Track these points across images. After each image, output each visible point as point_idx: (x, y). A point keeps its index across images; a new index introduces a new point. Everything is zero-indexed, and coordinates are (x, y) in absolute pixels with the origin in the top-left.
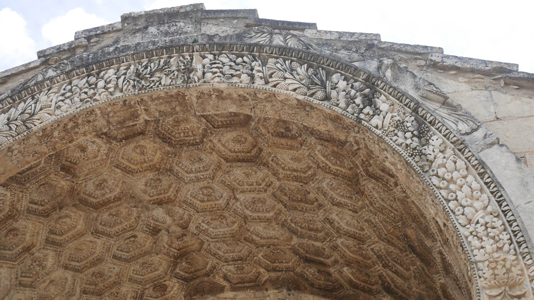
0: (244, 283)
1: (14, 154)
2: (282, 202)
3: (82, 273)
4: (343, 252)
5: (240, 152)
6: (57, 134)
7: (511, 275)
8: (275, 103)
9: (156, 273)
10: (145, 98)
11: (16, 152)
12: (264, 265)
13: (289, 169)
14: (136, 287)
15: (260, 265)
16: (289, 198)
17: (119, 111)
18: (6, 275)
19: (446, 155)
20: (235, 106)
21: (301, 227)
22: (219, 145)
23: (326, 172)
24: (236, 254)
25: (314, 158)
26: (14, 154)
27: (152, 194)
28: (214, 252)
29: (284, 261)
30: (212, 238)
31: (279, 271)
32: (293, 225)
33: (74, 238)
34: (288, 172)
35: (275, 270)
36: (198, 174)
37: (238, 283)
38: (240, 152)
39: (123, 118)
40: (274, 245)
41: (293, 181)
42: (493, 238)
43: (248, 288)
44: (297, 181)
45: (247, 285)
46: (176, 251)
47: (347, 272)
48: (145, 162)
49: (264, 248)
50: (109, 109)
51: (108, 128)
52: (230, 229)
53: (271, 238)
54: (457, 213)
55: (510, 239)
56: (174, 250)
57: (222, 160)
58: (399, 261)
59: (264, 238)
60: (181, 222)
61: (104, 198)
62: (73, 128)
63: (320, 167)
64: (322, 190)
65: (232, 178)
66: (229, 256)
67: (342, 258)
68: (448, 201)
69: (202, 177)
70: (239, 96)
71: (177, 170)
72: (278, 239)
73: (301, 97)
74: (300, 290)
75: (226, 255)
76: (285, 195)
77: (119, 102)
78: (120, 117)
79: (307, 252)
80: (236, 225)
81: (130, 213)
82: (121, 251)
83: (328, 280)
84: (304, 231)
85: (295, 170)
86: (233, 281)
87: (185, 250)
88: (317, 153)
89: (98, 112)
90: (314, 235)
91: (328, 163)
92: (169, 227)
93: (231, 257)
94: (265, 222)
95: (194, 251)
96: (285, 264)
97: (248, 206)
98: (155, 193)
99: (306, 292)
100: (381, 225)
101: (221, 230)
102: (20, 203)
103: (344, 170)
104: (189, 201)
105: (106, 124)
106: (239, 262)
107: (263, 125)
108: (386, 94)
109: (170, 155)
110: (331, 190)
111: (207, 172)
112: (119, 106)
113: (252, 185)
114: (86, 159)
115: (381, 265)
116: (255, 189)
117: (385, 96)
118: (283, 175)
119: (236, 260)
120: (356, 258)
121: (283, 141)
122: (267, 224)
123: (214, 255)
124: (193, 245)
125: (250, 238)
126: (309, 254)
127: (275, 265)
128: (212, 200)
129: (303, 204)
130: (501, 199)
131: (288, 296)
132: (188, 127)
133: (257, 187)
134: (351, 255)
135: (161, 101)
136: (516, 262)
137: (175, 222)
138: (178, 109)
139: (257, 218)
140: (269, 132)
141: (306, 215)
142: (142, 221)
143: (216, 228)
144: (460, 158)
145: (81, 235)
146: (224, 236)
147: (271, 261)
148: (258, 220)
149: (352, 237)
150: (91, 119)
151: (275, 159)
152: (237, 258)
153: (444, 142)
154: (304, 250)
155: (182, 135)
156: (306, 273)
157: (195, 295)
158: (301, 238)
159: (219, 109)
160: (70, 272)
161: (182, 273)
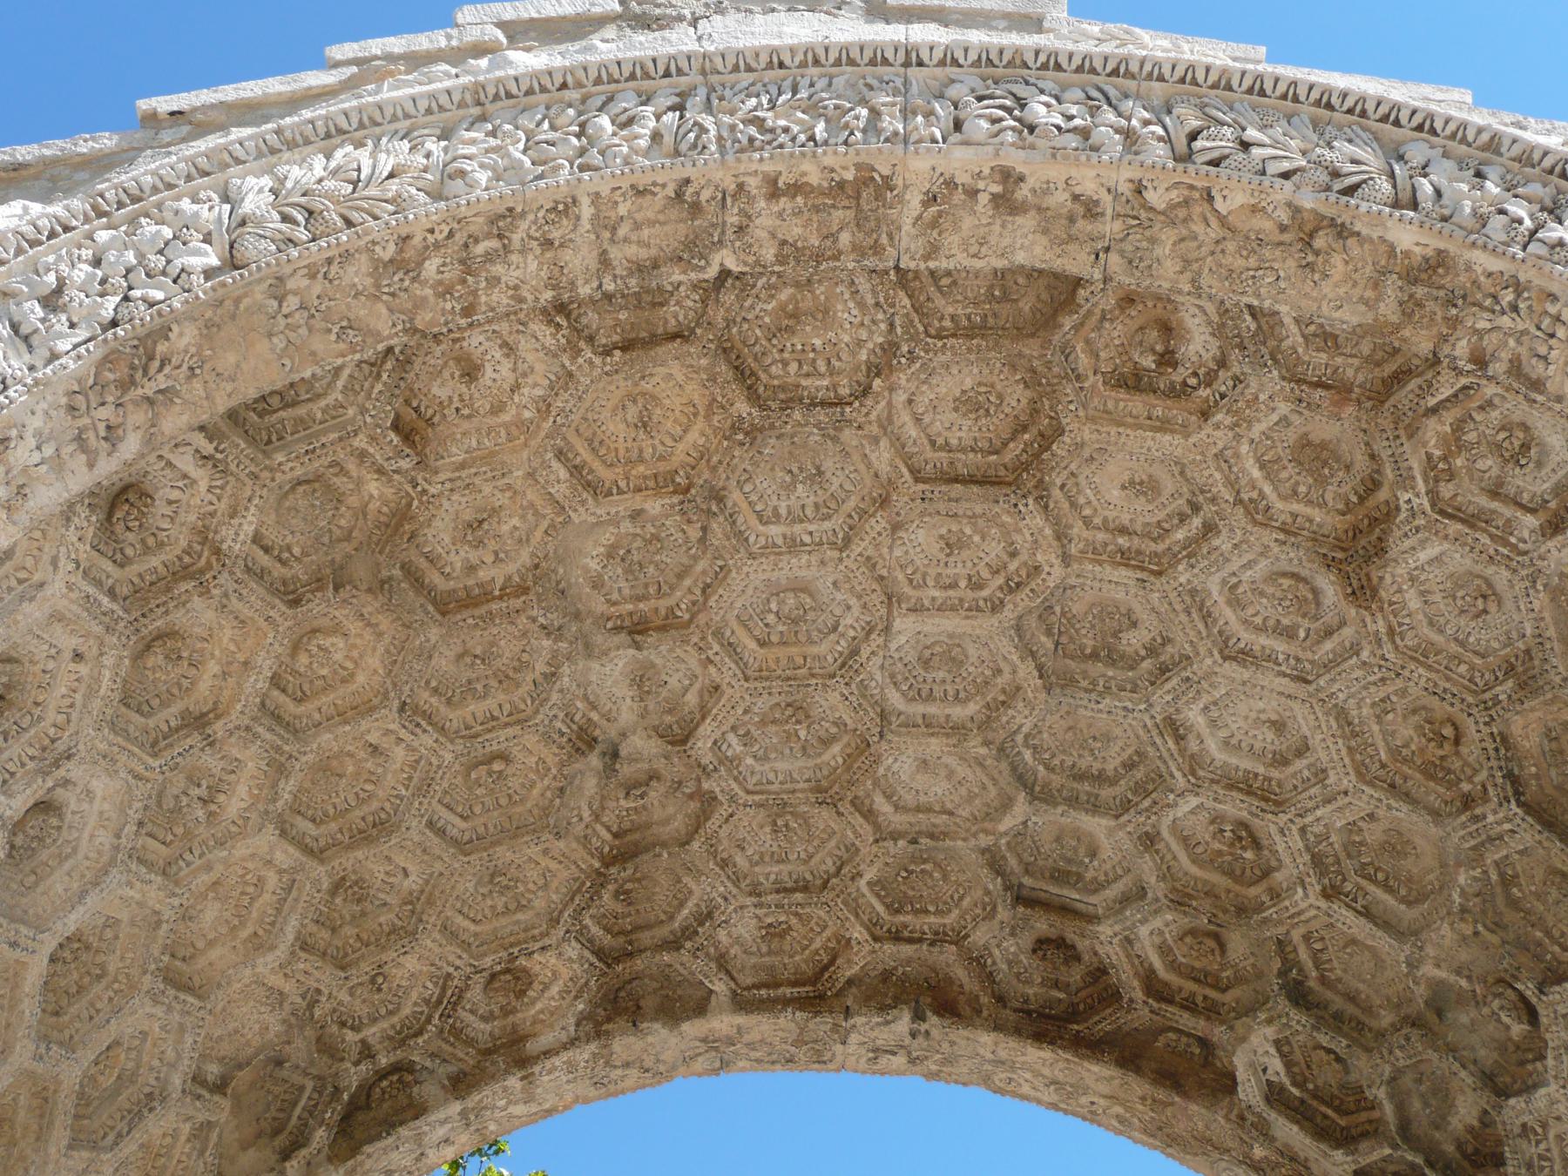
0: (777, 985)
1: (285, 310)
2: (1033, 654)
3: (322, 861)
4: (1169, 857)
5: (963, 450)
6: (434, 268)
8: (1198, 228)
9: (520, 916)
10: (753, 183)
11: (292, 302)
12: (865, 918)
13: (1105, 526)
15: (857, 916)
16: (1057, 644)
17: (652, 223)
18: (106, 806)
20: (1044, 240)
21: (1047, 767)
22: (905, 417)
23: (1255, 523)
24: (790, 867)
26: (285, 310)
27: (615, 596)
28: (725, 855)
29: (932, 909)
30: (748, 792)
31: (910, 941)
32: (1027, 755)
33: (342, 715)
34: (1101, 536)
35: (896, 937)
36: (798, 528)
37: (757, 986)
38: (963, 450)
39: (653, 252)
40: (932, 836)
43: (786, 1002)
44: (1127, 565)
45: (788, 991)
46: (608, 837)
47: (1147, 943)
48: (641, 460)
49: (901, 843)
50: (622, 210)
51: (595, 285)
52: (811, 763)
53: (929, 810)
57: (905, 470)
58: (1380, 876)
59: (906, 810)
60: (668, 719)
61: (471, 582)
62: (489, 257)
63: (1241, 501)
65: (898, 552)
66: (767, 876)
67: (1163, 878)
69: (807, 539)
70: (1076, 198)
71: (735, 505)
72: (951, 813)
74: (959, 1015)
75: (757, 869)
76: (1049, 633)
77: (664, 186)
78: (648, 246)
79: (1027, 872)
80: (836, 749)
81: (525, 657)
82: (448, 807)
83: (1056, 985)
85: (1123, 531)
86: (740, 977)
87: (637, 836)
89: (586, 211)
90: (1088, 794)
92: (624, 735)
93: (773, 877)
94: (947, 735)
95: (664, 845)
96: (932, 919)
98: (626, 592)
99: (978, 1021)
100: (1376, 728)
101: (782, 766)
102: (235, 522)
103: (1317, 515)
104: (728, 633)
105: (594, 265)
106: (799, 896)
107: (1087, 342)
109: (740, 437)
110: (1229, 603)
111: (827, 525)
112: (659, 200)
113: (954, 585)
114: (466, 412)
115: (1318, 888)
116: (961, 600)
118: (1081, 546)
119: (786, 890)
120: (1206, 882)
121: (1136, 404)
122: (953, 741)
123: (724, 864)
124: (666, 821)
125: (867, 802)
127: (901, 918)
128: (797, 643)
132: (818, 342)
133: (970, 594)
134: (1194, 870)
135: (799, 199)
138: (845, 238)
142: (561, 691)
143: (766, 758)
145: (365, 709)
146: (788, 786)
147: (888, 907)
149: (1240, 790)
150: (555, 235)
151: (1070, 483)
152: (790, 885)
154: (1021, 861)
155: (793, 367)
156: (990, 955)
157: (609, 1020)
159: (984, 250)
160: (291, 850)
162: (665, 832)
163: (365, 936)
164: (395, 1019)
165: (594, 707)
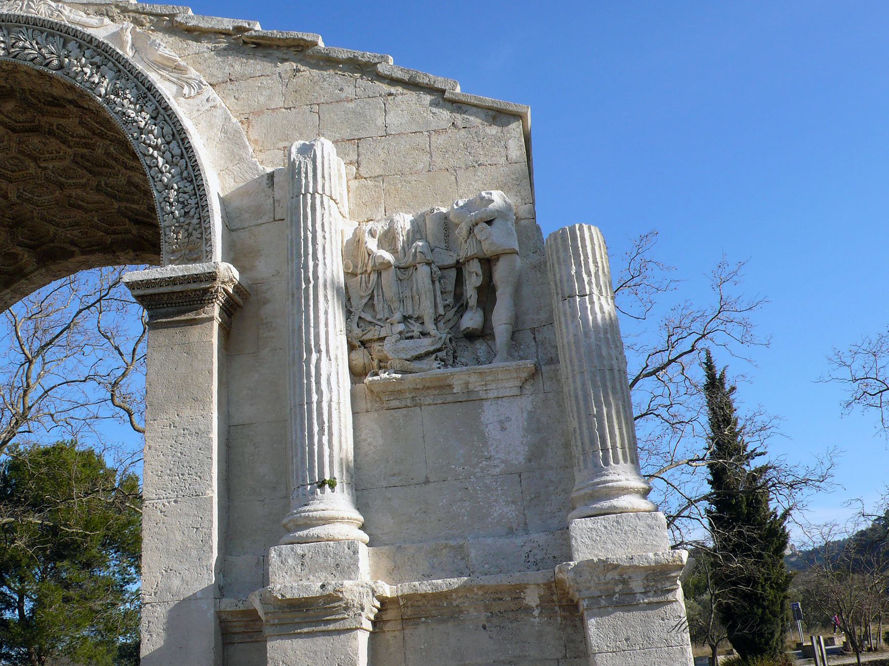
5: (25, 122)
7: (191, 238)
15: (98, 229)
19: (157, 122)
21: (118, 191)
25: (88, 125)
30: (38, 206)
32: (109, 189)
35: (114, 233)
37: (87, 247)
38: (25, 122)
41: (83, 148)
42: (183, 203)
44: (86, 148)
53: (98, 202)
54: (156, 180)
55: (197, 203)
59: (91, 203)
64: (112, 155)
66: (66, 222)
68: (150, 167)
72: (104, 203)
73: (37, 67)
75: (63, 221)
79: (136, 215)
84: (122, 195)
88: (89, 120)
91: (103, 129)
97: (61, 174)
108: (114, 60)
113: (52, 153)
117: (113, 63)
118: (73, 143)
126: (138, 216)
127: (114, 227)
129: (106, 170)
130: (195, 164)
131: (136, 257)
133: (57, 155)
136: (198, 225)
139: (72, 184)
140: (40, 102)
141: (110, 179)
143: (41, 196)
144: (168, 124)
148: (74, 187)
153: (157, 108)
158: (120, 201)
161: (26, 241)
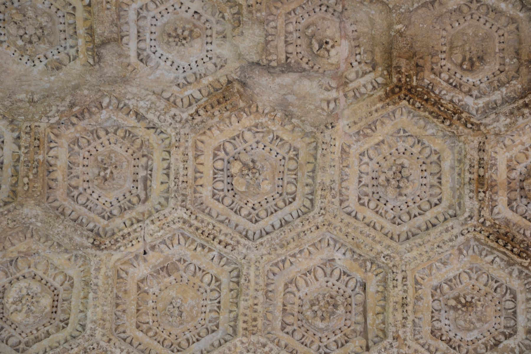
9: (446, 165)
14: (446, 236)
27: (72, 52)
46: (370, 77)
56: (362, 81)
95: (390, 26)
124: (372, 22)
137: (228, 33)
161: (497, 96)
162: (380, 20)
163: (378, 309)
164: (521, 297)
165: (199, 77)
